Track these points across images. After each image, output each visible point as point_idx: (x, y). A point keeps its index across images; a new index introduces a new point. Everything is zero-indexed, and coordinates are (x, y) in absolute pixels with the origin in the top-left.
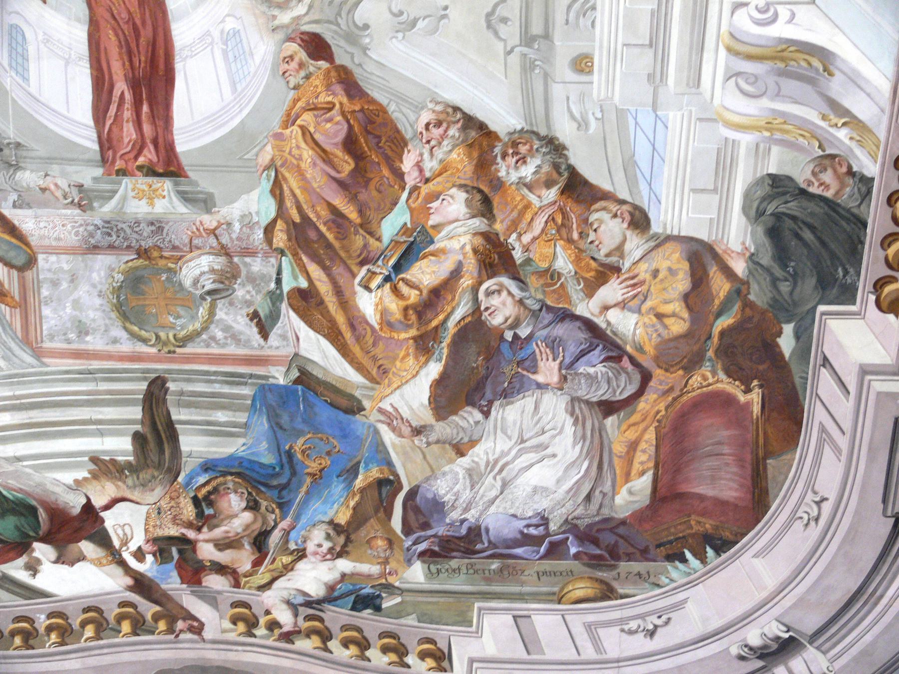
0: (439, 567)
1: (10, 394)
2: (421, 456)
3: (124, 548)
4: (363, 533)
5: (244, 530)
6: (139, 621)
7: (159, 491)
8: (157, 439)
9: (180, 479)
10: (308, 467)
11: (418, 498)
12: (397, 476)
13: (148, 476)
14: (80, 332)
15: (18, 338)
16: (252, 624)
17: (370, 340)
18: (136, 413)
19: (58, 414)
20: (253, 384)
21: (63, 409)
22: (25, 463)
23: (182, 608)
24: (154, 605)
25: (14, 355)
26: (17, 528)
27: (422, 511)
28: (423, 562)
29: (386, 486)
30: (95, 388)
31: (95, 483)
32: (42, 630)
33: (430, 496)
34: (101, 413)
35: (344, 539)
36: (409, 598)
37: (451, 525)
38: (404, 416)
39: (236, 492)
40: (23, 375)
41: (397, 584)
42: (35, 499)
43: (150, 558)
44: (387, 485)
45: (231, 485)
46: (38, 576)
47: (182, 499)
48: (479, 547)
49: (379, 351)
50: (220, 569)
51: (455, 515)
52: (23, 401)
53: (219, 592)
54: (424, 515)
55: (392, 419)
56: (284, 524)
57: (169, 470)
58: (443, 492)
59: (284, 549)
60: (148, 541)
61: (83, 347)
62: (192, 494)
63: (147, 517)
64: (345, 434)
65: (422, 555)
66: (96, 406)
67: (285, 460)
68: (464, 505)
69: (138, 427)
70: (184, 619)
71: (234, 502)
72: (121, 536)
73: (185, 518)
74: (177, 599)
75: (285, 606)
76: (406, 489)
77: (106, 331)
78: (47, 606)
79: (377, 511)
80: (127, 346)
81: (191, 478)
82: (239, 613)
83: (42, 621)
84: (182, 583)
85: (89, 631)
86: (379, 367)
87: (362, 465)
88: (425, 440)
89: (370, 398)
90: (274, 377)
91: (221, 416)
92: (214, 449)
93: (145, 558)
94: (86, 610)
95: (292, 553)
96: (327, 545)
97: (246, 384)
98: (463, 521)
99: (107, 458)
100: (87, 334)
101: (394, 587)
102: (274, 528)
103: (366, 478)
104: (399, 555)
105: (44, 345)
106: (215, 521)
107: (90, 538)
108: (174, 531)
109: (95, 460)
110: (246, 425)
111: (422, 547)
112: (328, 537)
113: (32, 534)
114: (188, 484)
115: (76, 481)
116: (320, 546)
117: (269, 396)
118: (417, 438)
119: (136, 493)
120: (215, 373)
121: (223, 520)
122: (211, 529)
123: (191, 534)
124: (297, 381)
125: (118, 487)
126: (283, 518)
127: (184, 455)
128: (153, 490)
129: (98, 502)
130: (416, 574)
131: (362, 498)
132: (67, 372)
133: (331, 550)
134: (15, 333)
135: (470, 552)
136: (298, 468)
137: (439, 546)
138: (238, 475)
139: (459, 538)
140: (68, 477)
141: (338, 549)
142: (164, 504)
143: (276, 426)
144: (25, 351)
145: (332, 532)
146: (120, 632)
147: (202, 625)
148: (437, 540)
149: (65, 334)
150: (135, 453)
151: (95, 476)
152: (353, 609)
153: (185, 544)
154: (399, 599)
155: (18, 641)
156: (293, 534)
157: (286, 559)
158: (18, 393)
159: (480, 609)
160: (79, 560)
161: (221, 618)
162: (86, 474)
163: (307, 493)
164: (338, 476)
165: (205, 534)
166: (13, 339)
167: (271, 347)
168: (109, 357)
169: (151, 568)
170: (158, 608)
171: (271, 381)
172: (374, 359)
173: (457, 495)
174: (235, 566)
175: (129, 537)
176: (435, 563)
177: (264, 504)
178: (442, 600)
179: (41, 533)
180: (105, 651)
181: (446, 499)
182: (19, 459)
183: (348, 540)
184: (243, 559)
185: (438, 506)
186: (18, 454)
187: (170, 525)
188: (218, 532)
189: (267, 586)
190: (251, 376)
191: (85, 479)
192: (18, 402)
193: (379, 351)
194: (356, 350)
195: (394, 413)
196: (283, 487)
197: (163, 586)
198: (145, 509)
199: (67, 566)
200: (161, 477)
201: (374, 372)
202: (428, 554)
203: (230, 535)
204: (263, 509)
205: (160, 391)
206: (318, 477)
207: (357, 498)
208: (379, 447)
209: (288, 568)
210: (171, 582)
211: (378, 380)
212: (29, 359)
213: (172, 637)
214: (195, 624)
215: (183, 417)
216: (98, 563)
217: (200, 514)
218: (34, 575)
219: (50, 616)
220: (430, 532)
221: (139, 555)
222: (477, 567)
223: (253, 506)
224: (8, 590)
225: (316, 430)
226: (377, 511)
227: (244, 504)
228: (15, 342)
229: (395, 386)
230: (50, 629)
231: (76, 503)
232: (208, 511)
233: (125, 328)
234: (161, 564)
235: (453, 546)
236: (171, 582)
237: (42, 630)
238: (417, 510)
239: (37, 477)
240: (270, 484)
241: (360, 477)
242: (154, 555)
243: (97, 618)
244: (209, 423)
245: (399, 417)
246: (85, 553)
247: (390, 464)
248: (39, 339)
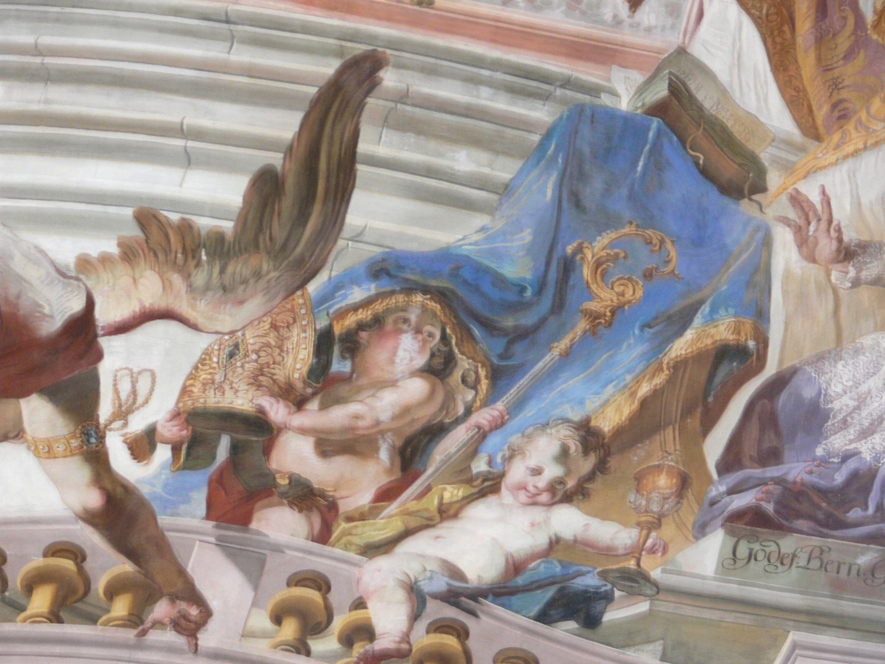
0: (756, 547)
2: (831, 306)
3: (117, 424)
4: (637, 457)
5: (395, 418)
6: (74, 591)
7: (254, 306)
8: (308, 185)
9: (313, 287)
10: (591, 297)
11: (783, 397)
12: (763, 342)
13: (247, 272)
16: (313, 624)
17: (843, 43)
18: (285, 125)
20: (563, 101)
23: (182, 573)
24: (122, 558)
27: (781, 420)
28: (730, 532)
29: (731, 361)
33: (808, 393)
35: (597, 460)
36: (666, 606)
37: (823, 462)
38: (836, 216)
39: (418, 331)
41: (656, 574)
43: (163, 453)
44: (735, 359)
45: (413, 317)
47: (295, 331)
48: (855, 514)
49: (849, 72)
50: (304, 496)
51: (838, 442)
52: (48, 60)
53: (278, 549)
54: (778, 433)
55: (807, 217)
56: (483, 417)
57: (300, 262)
58: (839, 389)
59: (460, 471)
60: (176, 415)
62: (322, 323)
63: (202, 361)
64: (702, 237)
65: (737, 517)
67: (553, 275)
68: (866, 423)
69: (276, 159)
70: (174, 598)
71: (404, 354)
72: (123, 396)
73: (280, 375)
75: (401, 595)
76: (771, 370)
79: (688, 411)
84: (208, 517)
86: (834, 106)
87: (706, 308)
88: (852, 272)
89: (787, 168)
90: (614, 93)
91: (464, 161)
92: (414, 231)
93: (152, 447)
95: (470, 481)
96: (552, 471)
97: (545, 97)
98: (846, 457)
99: (174, 217)
101: (646, 578)
102: (458, 421)
103: (699, 338)
104: (690, 513)
106: (343, 390)
107: (53, 394)
108: (242, 400)
109: (147, 218)
110: (505, 190)
111: (741, 501)
112: (564, 456)
114: (326, 298)
116: (537, 472)
117: (586, 131)
118: (839, 266)
119: (202, 305)
120: (495, 65)
121: (360, 390)
122: (324, 407)
123: (278, 412)
124: (659, 110)
125: (167, 285)
126: (488, 402)
127: (346, 232)
128: (241, 302)
129: (104, 315)
130: (703, 558)
131: (670, 381)
133: (552, 488)
135: (832, 523)
136: (572, 297)
137: (777, 503)
138: (441, 295)
139: (823, 492)
140: (66, 249)
141: (571, 483)
142: (251, 339)
143: (570, 197)
145: (574, 446)
146: (22, 609)
147: (207, 613)
148: (777, 490)
151: (129, 254)
152: (544, 617)
153: (258, 430)
154: (643, 607)
156: (493, 441)
157: (452, 493)
159: (795, 646)
161: (255, 604)
162: (111, 247)
163: (567, 355)
164: (644, 326)
165: (313, 416)
167: (636, 26)
169: (156, 476)
170: (126, 567)
171: (605, 100)
172: (835, 85)
173: (861, 402)
174: (337, 495)
175: (140, 400)
176: (753, 538)
177: (464, 364)
178: (730, 618)
181: (836, 405)
183: (601, 467)
184: (358, 482)
185: (815, 418)
187: (243, 387)
188: (338, 416)
189: (385, 547)
190: (567, 83)
191: (105, 260)
193: (849, 72)
194: (807, 62)
195: (819, 207)
196: (522, 335)
197: (164, 520)
198: (200, 343)
200: (273, 274)
201: (821, 113)
202: (747, 518)
203: (361, 423)
204: (457, 375)
205: (360, 84)
206: (605, 325)
207: (659, 380)
208: (758, 276)
209: (447, 513)
211: (822, 130)
213: (130, 634)
215: (382, 151)
217: (320, 372)
220: (773, 472)
221: (142, 446)
222: (834, 556)
223: (438, 369)
225: (648, 220)
226: (688, 411)
227: (421, 361)
229: (849, 148)
231: (56, 307)
232: (339, 366)
234: (185, 468)
235: (804, 507)
238: (770, 422)
240: (486, 322)
241: (689, 334)
242: (176, 449)
244: (430, 172)
245: (825, 217)
246: (26, 425)
247: (761, 315)
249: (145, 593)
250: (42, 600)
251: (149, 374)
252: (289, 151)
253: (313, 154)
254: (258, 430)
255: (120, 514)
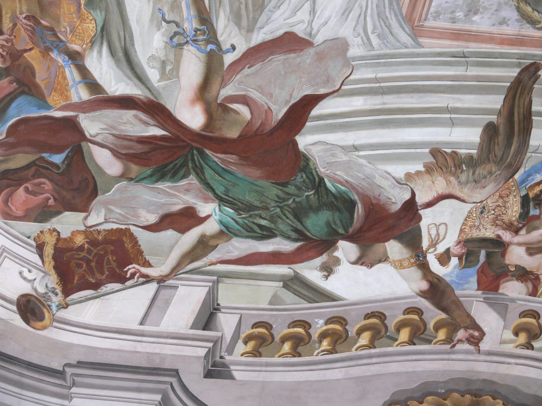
1: (372, 76)
3: (432, 250)
6: (419, 329)
7: (490, 188)
9: (517, 176)
13: (485, 173)
14: (470, 11)
15: (401, 14)
18: (496, 102)
19: (413, 100)
21: (422, 95)
22: (362, 153)
23: (469, 316)
24: (440, 312)
25: (391, 33)
26: (328, 224)
30: (464, 73)
31: (427, 177)
32: (315, 336)
34: (460, 100)
40: (393, 56)
42: (358, 193)
43: (454, 261)
46: (332, 277)
47: (511, 197)
50: (523, 274)
53: (513, 300)
57: (510, 165)
60: (459, 243)
61: (467, 27)
62: (523, 193)
63: (468, 217)
66: (457, 93)
69: (493, 118)
70: (466, 328)
72: (433, 237)
73: (506, 218)
74: (466, 305)
77: (497, 10)
78: (329, 309)
80: (514, 28)
81: (529, 176)
82: (526, 323)
83: (319, 326)
84: (478, 289)
85: (365, 339)
93: (449, 259)
94: (368, 316)
99: (449, 151)
100: (476, 13)
105: (427, 24)
107: (399, 238)
108: (489, 233)
109: (436, 152)
113: (341, 231)
114: (523, 181)
115: (409, 176)
119: (466, 190)
122: (528, 232)
123: (506, 236)
125: (448, 182)
127: (530, 149)
128: (484, 187)
129: (421, 199)
132: (440, 54)
134: (400, 9)
140: (399, 170)
142: (490, 203)
144: (404, 29)
146: (396, 340)
147: (483, 334)
149: (453, 12)
150: (481, 147)
151: (429, 170)
153: (498, 246)
155: (287, 347)
158: (380, 75)
160: (380, 261)
161: (504, 328)
162: (421, 168)
165: (523, 237)
166: (396, 15)
168: (490, 39)
169: (452, 272)
170: (443, 316)
174: (538, 273)
175: (441, 238)
179: (351, 230)
180: (374, 360)
182: (356, 148)
186: (357, 143)
187: (489, 226)
191: (418, 173)
192: (378, 85)
197: (458, 292)
198: (467, 207)
199: (365, 268)
200: (499, 172)
205: (530, 79)
210: (467, 290)
212: (405, 38)
213: (448, 347)
214: (476, 334)
216: (399, 265)
217: (525, 216)
218: (327, 277)
219: (328, 322)
224: (296, 293)
228: (398, 20)
230: (323, 336)
231: (397, 198)
233: (518, 9)
234: (464, 267)
236: (467, 290)
237: (315, 336)
239: (369, 169)
242: (460, 258)
243: (378, 326)
248: (423, 16)
249: (452, 327)
250: (404, 335)
251: (445, 224)
252: (500, 113)
253: (511, 114)
254: (498, 246)
255: (437, 291)
